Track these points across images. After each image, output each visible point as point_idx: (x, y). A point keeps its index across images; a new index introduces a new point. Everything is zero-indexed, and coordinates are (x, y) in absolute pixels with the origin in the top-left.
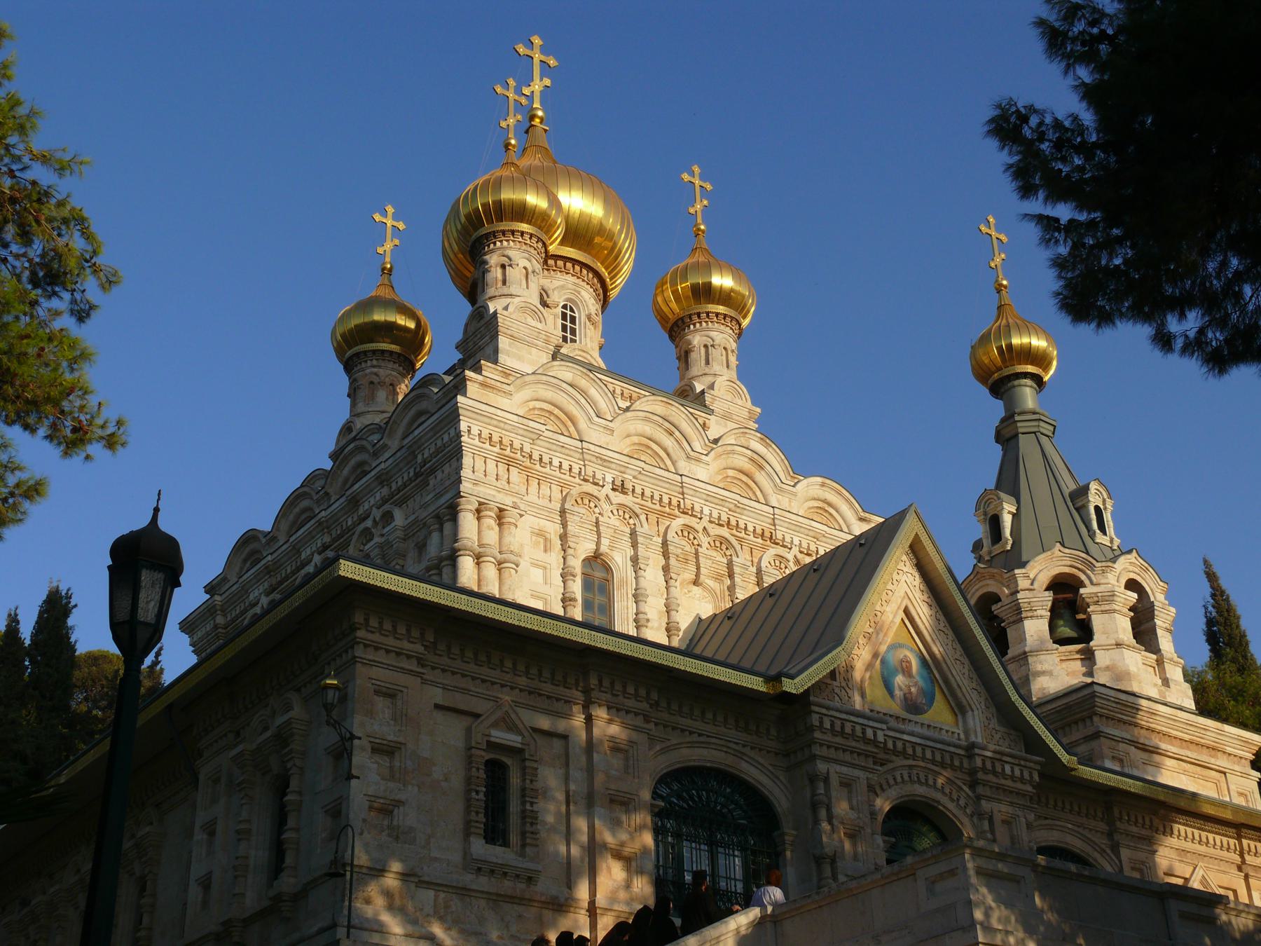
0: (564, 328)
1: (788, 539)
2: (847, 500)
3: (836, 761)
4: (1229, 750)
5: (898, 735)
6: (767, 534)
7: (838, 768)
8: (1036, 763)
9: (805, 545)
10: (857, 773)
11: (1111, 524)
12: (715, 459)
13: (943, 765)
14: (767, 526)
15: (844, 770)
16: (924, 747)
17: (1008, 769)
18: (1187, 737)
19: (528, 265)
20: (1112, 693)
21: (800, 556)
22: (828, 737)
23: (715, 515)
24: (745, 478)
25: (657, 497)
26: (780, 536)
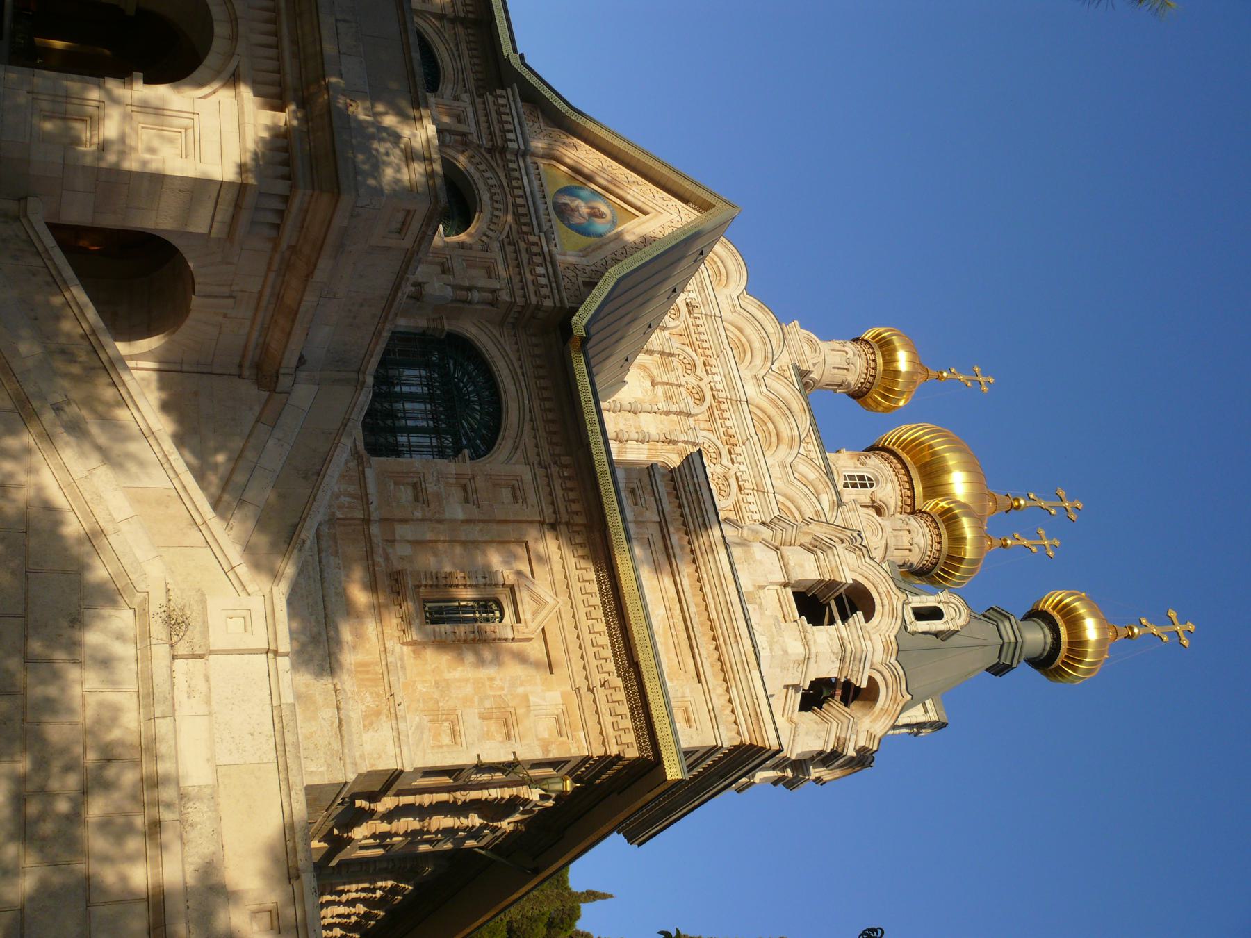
0: (851, 477)
1: (740, 459)
2: (734, 256)
3: (474, 107)
4: (733, 690)
5: (523, 172)
6: (732, 440)
7: (470, 109)
8: (561, 301)
9: (745, 477)
10: (473, 124)
11: (924, 598)
12: (767, 397)
13: (517, 215)
14: (739, 438)
15: (471, 115)
16: (524, 196)
17: (540, 270)
18: (714, 616)
19: (851, 354)
20: (702, 479)
21: (732, 472)
22: (492, 108)
23: (719, 386)
24: (774, 439)
25: (702, 337)
26: (738, 450)
